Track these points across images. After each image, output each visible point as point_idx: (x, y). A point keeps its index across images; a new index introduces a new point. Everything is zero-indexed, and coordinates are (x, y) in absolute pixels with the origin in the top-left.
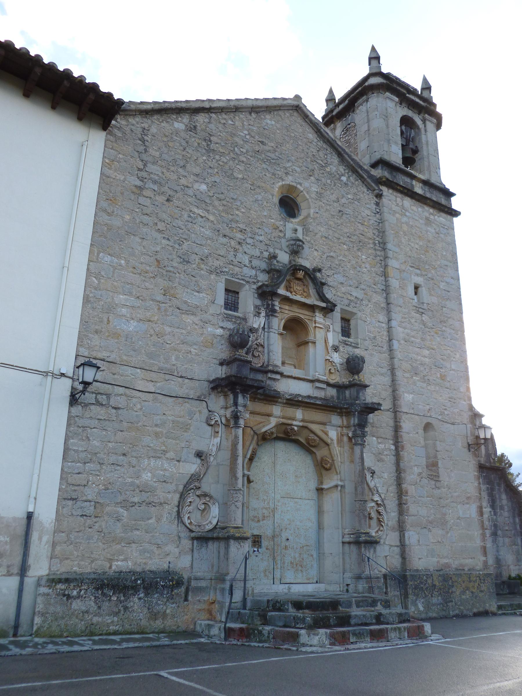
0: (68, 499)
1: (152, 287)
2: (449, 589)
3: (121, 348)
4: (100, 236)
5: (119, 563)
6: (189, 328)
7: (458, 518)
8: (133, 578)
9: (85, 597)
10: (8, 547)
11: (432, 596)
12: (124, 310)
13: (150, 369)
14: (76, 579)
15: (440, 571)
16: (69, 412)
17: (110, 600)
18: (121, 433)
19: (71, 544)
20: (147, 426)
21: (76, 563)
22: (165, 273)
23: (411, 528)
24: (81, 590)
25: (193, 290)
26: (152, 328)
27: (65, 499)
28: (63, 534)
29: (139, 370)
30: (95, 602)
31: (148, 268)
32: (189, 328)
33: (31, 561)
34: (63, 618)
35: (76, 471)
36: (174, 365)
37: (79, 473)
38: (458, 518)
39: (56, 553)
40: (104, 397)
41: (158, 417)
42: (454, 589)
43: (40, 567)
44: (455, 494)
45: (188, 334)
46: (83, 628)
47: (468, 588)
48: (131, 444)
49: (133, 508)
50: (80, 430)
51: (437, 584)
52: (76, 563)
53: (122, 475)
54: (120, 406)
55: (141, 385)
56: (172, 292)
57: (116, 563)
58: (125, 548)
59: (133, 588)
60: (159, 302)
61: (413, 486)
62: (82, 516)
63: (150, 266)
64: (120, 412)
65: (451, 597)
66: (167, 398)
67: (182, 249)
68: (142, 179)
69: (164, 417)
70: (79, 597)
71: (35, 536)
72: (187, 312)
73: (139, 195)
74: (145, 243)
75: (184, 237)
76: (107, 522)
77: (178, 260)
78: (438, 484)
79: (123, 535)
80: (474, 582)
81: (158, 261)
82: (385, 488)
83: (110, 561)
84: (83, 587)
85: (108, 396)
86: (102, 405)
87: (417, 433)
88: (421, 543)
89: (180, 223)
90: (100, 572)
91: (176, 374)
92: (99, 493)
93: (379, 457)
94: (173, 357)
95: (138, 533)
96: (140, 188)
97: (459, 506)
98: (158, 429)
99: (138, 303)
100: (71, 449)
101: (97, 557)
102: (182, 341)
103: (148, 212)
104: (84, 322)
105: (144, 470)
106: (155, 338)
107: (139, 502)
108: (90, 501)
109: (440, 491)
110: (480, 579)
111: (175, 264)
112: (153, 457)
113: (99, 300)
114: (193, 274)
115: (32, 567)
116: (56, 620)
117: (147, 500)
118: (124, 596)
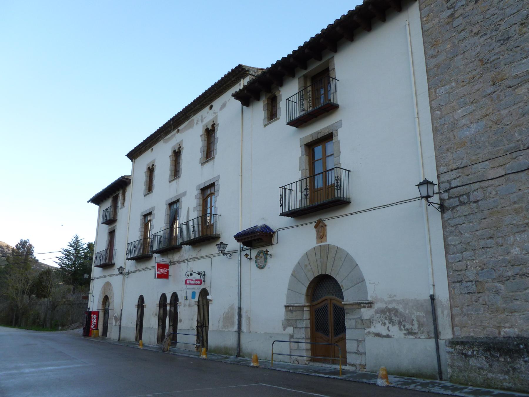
0: (456, 282)
1: (482, 85)
3: (469, 152)
4: (434, 77)
5: (507, 330)
6: (525, 97)
8: (515, 343)
9: (478, 357)
10: (425, 320)
12: (464, 121)
13: (497, 156)
14: (468, 342)
16: (442, 218)
17: (498, 360)
18: (484, 220)
19: (465, 315)
20: (505, 207)
21: (472, 329)
22: (489, 65)
24: (473, 351)
25: (520, 60)
26: (490, 120)
27: (453, 282)
28: (458, 309)
29: (487, 163)
30: (486, 361)
31: (474, 73)
32: (525, 97)
33: (440, 328)
34: (466, 371)
35: (458, 260)
36: (518, 141)
37: (459, 261)
39: (456, 322)
40: (465, 197)
41: (514, 195)
43: (446, 334)
45: (526, 104)
46: (482, 381)
48: (495, 227)
49: (508, 281)
50: (453, 229)
52: (472, 329)
53: (493, 255)
54: (479, 198)
55: (492, 174)
56: (500, 77)
57: (503, 330)
58: (509, 317)
59: (517, 351)
60: (491, 94)
62: (468, 293)
63: (475, 70)
64: (480, 203)
66: (520, 174)
67: (500, 32)
68: (452, 7)
69: (521, 193)
70: (473, 356)
71: (439, 311)
72: (519, 85)
73: (453, 21)
74: (466, 54)
75: (499, 19)
76: (488, 296)
77: (499, 44)
79: (504, 305)
81: (481, 60)
83: (499, 328)
84: (475, 349)
85: (468, 194)
86: (464, 203)
89: (491, 11)
90: (491, 337)
91: (522, 148)
92: (477, 274)
94: (516, 134)
95: (518, 302)
96: (452, 15)
98: (517, 206)
99: (472, 108)
100: (450, 245)
101: (487, 325)
102: (521, 114)
103: (463, 28)
104: (438, 148)
105: (512, 246)
106: (495, 127)
107: (513, 276)
108: (472, 281)
111: (496, 51)
112: (517, 232)
113: (444, 124)
114: (516, 45)
115: (442, 332)
116: (461, 371)
117: (521, 272)
118: (510, 358)
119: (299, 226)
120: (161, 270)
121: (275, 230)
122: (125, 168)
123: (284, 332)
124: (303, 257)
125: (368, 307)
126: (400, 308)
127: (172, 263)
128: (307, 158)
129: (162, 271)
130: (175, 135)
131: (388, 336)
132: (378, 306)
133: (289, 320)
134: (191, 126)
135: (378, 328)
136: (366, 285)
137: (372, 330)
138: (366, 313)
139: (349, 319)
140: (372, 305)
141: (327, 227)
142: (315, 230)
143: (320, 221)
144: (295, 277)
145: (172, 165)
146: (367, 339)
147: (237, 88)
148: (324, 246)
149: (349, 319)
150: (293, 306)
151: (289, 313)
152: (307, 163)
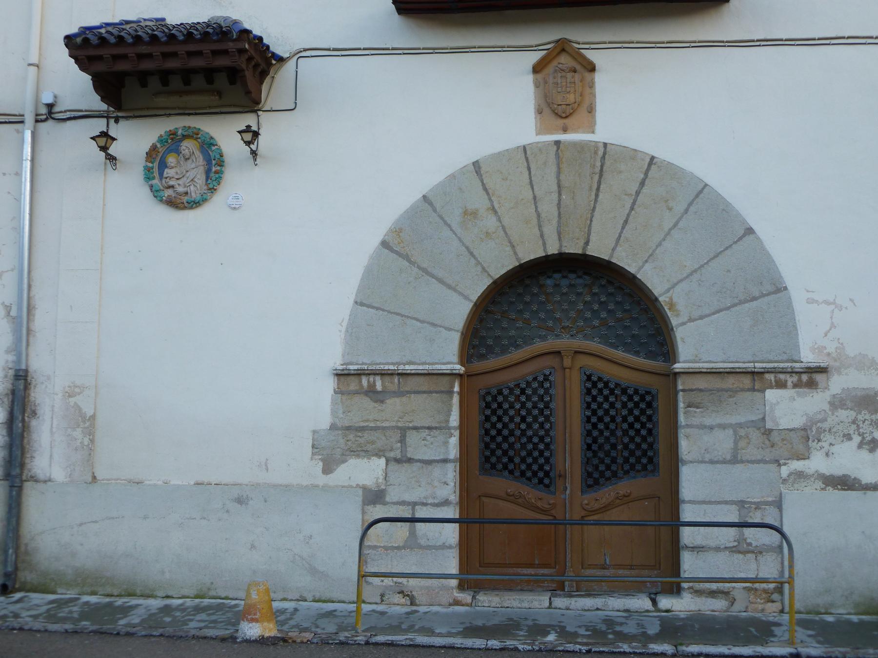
119: (434, 51)
121: (278, 49)
123: (322, 480)
124: (452, 177)
125: (795, 386)
133: (362, 429)
135: (848, 458)
136: (789, 305)
137: (817, 463)
138: (787, 408)
139: (702, 427)
140: (819, 377)
141: (600, 79)
142: (529, 80)
143: (562, 47)
144: (407, 258)
146: (791, 498)
148: (580, 147)
149: (702, 427)
150: (383, 374)
151: (367, 402)
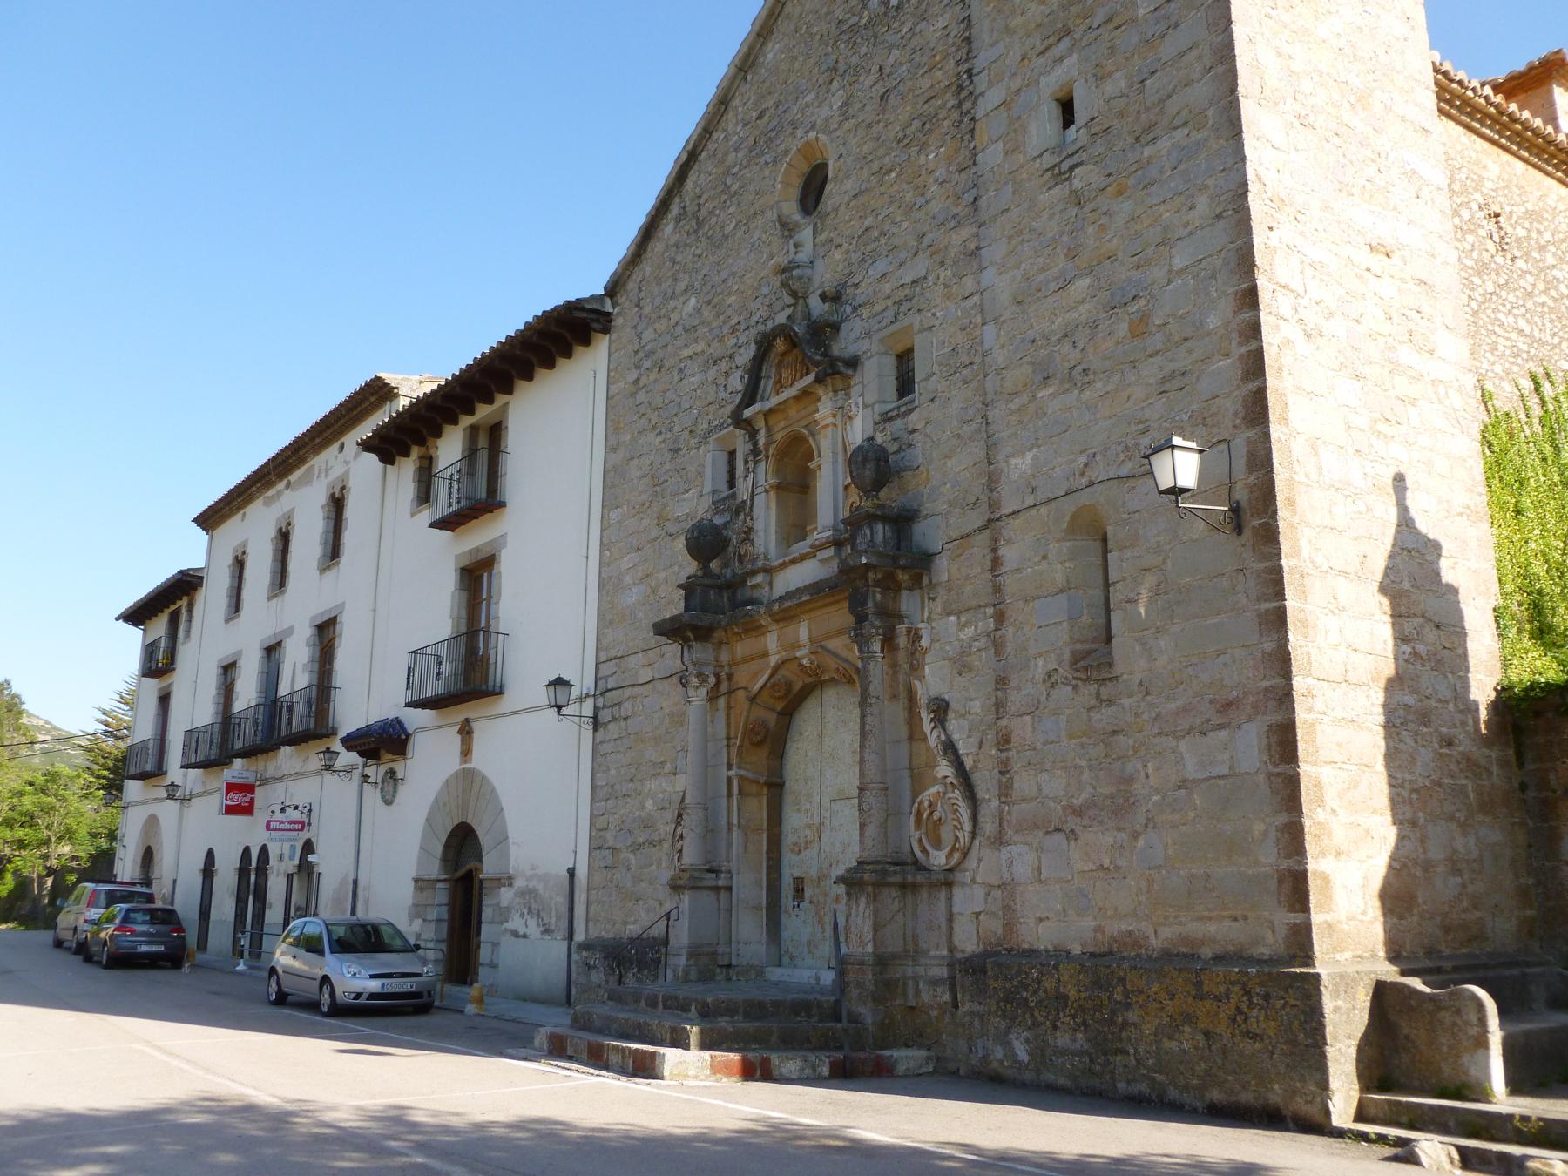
2: (1113, 1013)
7: (1183, 784)
11: (1055, 1027)
15: (1102, 955)
23: (1016, 838)
38: (1183, 784)
42: (1132, 1016)
44: (1172, 706)
47: (1189, 1019)
51: (1072, 994)
61: (1028, 718)
65: (1121, 1040)
78: (1105, 692)
80: (1218, 998)
82: (974, 741)
87: (1044, 558)
88: (1043, 877)
93: (961, 664)
97: (1183, 746)
109: (1113, 708)
110: (1248, 993)
111: (668, 466)
120: (236, 797)
122: (190, 550)
126: (540, 887)
127: (263, 781)
128: (465, 595)
129: (238, 798)
130: (279, 493)
131: (525, 936)
132: (519, 883)
134: (306, 481)
137: (510, 925)
142: (459, 737)
145: (274, 560)
147: (365, 430)
152: (464, 604)
